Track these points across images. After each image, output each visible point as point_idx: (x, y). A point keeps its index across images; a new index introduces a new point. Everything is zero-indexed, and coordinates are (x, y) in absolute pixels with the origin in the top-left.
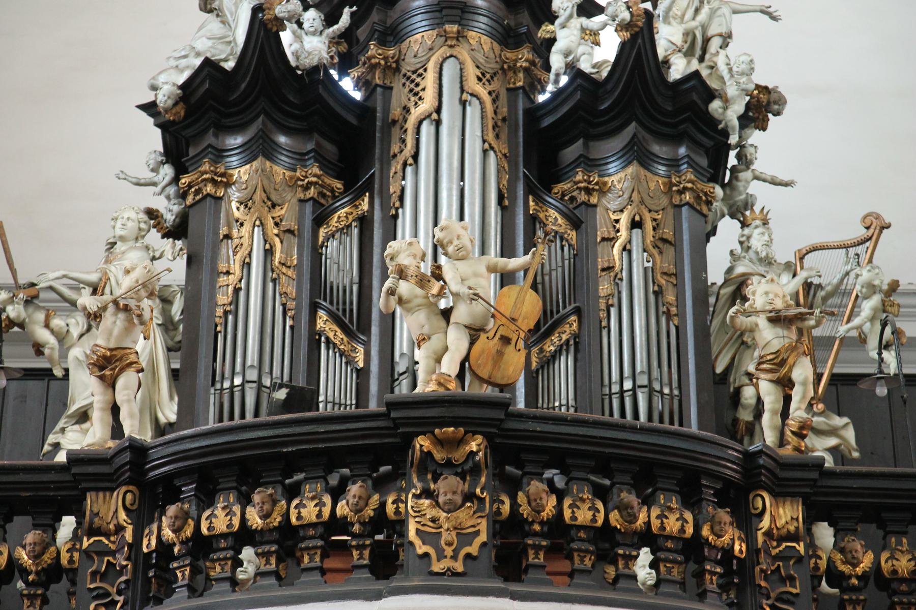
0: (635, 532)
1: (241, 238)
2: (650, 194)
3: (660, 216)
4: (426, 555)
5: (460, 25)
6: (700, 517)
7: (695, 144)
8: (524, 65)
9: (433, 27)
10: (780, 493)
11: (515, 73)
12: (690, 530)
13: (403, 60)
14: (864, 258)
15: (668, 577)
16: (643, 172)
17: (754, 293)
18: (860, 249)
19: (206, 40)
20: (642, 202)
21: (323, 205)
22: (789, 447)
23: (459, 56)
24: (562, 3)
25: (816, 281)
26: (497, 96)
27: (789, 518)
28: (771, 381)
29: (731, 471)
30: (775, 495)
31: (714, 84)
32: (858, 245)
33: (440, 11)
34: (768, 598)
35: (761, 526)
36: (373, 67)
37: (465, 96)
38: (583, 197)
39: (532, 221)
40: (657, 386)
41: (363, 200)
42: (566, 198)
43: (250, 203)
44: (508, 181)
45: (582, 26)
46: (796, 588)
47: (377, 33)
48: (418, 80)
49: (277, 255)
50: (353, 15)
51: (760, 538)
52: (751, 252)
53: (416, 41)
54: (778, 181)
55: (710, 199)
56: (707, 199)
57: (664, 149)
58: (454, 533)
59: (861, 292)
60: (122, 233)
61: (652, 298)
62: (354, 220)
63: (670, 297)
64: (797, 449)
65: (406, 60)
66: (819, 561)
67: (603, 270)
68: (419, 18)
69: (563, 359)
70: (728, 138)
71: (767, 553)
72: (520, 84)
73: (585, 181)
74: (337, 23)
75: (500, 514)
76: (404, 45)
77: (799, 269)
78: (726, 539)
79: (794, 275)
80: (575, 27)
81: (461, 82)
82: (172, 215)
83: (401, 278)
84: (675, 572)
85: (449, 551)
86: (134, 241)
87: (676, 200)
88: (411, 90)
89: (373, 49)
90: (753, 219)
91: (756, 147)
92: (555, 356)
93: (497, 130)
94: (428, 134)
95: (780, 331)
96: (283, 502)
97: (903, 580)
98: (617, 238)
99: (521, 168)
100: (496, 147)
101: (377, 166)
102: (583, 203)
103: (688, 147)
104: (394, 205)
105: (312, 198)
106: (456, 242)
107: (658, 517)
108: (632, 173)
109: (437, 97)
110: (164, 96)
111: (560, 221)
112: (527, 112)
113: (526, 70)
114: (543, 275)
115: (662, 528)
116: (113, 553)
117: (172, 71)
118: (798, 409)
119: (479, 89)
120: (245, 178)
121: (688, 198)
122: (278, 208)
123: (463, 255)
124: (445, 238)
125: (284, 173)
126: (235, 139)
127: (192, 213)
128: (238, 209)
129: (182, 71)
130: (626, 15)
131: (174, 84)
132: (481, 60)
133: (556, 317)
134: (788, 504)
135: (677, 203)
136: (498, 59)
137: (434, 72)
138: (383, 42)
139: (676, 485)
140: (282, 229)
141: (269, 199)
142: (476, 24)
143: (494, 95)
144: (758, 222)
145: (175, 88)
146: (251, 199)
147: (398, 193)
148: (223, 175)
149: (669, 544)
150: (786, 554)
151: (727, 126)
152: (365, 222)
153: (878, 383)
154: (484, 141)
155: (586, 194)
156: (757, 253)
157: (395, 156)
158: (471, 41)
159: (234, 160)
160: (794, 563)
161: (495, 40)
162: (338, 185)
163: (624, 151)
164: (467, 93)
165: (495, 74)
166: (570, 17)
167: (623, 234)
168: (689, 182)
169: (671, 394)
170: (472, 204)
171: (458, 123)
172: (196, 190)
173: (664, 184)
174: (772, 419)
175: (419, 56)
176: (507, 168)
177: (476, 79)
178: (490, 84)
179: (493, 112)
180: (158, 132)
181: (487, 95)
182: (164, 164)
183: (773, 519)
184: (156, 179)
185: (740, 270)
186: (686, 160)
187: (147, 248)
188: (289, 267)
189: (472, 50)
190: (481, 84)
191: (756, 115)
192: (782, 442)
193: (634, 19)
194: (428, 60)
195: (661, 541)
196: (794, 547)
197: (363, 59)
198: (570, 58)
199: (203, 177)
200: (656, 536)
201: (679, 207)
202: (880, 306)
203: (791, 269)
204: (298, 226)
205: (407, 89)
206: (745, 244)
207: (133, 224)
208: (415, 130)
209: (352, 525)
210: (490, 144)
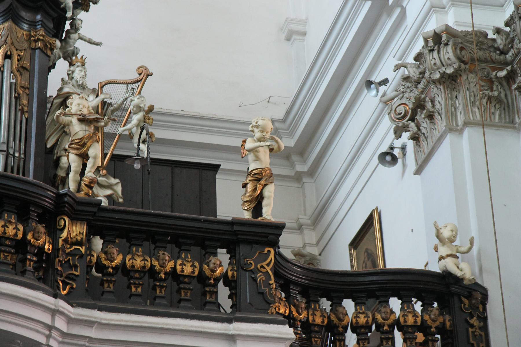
2: (18, 40)
3: (22, 54)
6: (27, 228)
7: (46, 14)
10: (74, 219)
12: (20, 235)
14: (136, 91)
15: (5, 261)
16: (14, 26)
17: (71, 104)
18: (134, 86)
20: (12, 44)
22: (83, 193)
25: (109, 101)
27: (78, 233)
28: (76, 155)
29: (48, 203)
30: (72, 219)
32: (134, 83)
34: (61, 276)
35: (62, 236)
40: (11, 152)
46: (78, 272)
52: (73, 80)
54: (93, 41)
55: (52, 47)
56: (51, 47)
57: (28, 15)
59: (133, 109)
61: (13, 100)
63: (24, 101)
64: (87, 194)
66: (92, 258)
70: (66, 13)
71: (64, 251)
77: (100, 93)
78: (41, 242)
79: (97, 96)
84: (9, 258)
87: (33, 45)
90: (77, 62)
91: (82, 21)
95: (84, 127)
97: (137, 271)
103: (42, 16)
108: (7, 27)
118: (90, 172)
121: (40, 45)
134: (78, 225)
135: (33, 47)
139: (15, 209)
144: (79, 64)
149: (8, 242)
150: (74, 253)
151: (65, 6)
153: (136, 162)
156: (77, 81)
160: (78, 258)
163: (4, 13)
168: (41, 35)
169: (19, 157)
173: (26, 35)
174: (74, 176)
183: (69, 232)
185: (66, 90)
186: (40, 23)
191: (83, 2)
192: (79, 190)
196: (79, 249)
201: (34, 49)
202: (143, 119)
206: (70, 76)
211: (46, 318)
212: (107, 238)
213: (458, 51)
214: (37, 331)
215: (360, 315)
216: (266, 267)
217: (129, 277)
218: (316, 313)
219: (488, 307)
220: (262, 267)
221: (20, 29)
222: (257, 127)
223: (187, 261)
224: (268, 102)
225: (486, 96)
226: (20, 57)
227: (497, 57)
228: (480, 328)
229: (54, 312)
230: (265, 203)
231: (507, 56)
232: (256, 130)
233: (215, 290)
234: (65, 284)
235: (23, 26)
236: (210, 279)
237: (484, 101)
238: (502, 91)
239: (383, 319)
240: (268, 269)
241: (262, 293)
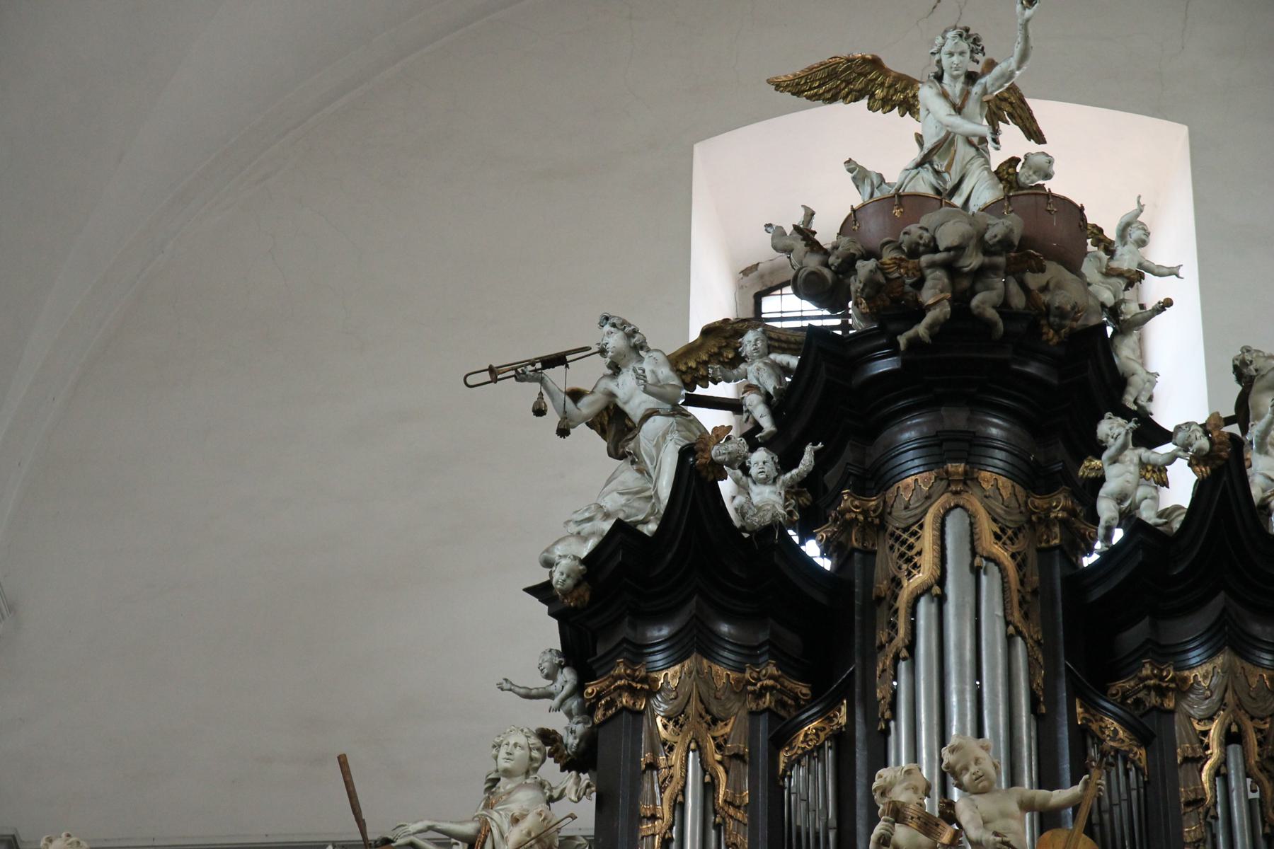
1: (670, 767)
2: (1252, 694)
3: (1268, 726)
5: (967, 463)
8: (1060, 515)
9: (929, 467)
11: (1047, 527)
13: (890, 513)
16: (1238, 662)
19: (618, 495)
20: (1240, 705)
21: (783, 719)
23: (968, 506)
24: (1111, 429)
26: (1024, 560)
33: (940, 445)
36: (847, 525)
37: (978, 561)
38: (1154, 699)
39: (1082, 736)
41: (839, 711)
42: (1129, 702)
43: (682, 719)
44: (1044, 680)
45: (1140, 459)
47: (852, 478)
48: (912, 540)
49: (722, 791)
50: (817, 454)
53: (908, 486)
57: (1269, 629)
60: (508, 765)
62: (827, 739)
65: (894, 514)
67: (1188, 804)
68: (910, 455)
72: (1057, 541)
73: (1155, 676)
74: (797, 466)
80: (1131, 461)
81: (972, 542)
82: (575, 738)
83: (897, 821)
86: (524, 777)
88: (902, 555)
89: (847, 500)
93: (1025, 607)
98: (1207, 758)
99: (1063, 662)
100: (1025, 631)
101: (857, 661)
102: (1154, 708)
104: (883, 716)
105: (768, 709)
106: (973, 769)
108: (1223, 664)
109: (939, 563)
110: (562, 574)
111: (1121, 734)
112: (1066, 580)
113: (1063, 523)
114: (1100, 812)
117: (572, 540)
119: (997, 550)
120: (674, 683)
122: (721, 724)
123: (984, 787)
124: (957, 763)
125: (727, 674)
126: (660, 630)
127: (601, 734)
128: (665, 726)
129: (585, 539)
130: (1204, 443)
131: (575, 558)
132: (999, 511)
136: (1023, 509)
137: (933, 529)
138: (861, 491)
140: (727, 753)
141: (708, 711)
142: (990, 461)
143: (1019, 558)
145: (577, 563)
146: (683, 712)
147: (888, 699)
148: (644, 680)
152: (842, 741)
154: (1007, 623)
155: (1157, 695)
157: (882, 647)
158: (985, 485)
159: (659, 659)
161: (1017, 483)
162: (803, 689)
164: (981, 556)
165: (1019, 529)
166: (1124, 447)
167: (1215, 752)
170: (994, 713)
171: (970, 599)
172: (607, 702)
175: (911, 507)
176: (1042, 663)
177: (993, 537)
178: (1013, 544)
179: (1018, 583)
180: (556, 622)
181: (1009, 558)
182: (562, 667)
184: (552, 689)
187: (542, 785)
188: (738, 807)
189: (986, 497)
190: (1000, 544)
193: (1216, 448)
194: (925, 512)
197: (833, 515)
198: (1127, 504)
199: (616, 684)
204: (750, 749)
205: (896, 554)
207: (523, 752)
208: (909, 611)
210: (1016, 628)
221: (1254, 665)
226: (1264, 734)
235: (1259, 657)
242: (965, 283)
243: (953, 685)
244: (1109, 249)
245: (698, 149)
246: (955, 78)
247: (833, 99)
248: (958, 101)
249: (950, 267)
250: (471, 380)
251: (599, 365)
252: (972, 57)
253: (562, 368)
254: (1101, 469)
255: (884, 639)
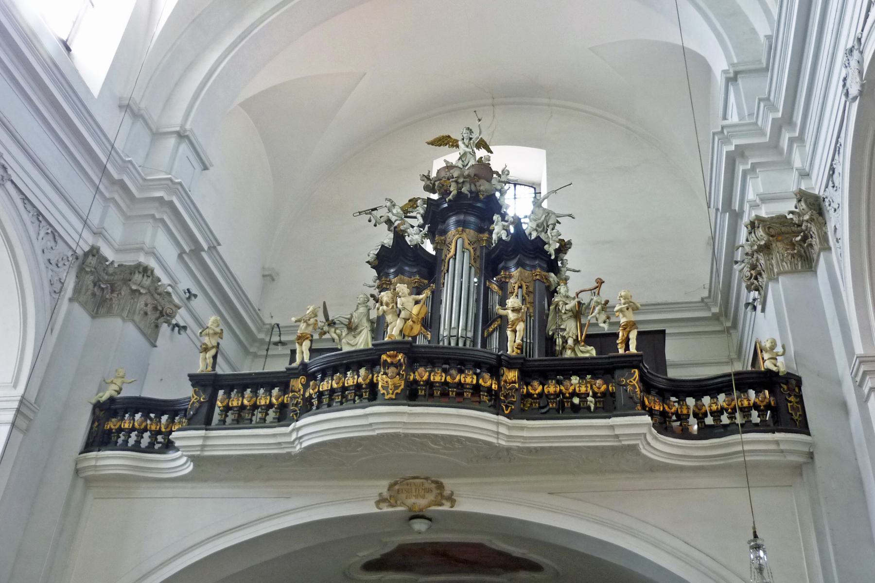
0: (455, 383)
4: (384, 394)
10: (510, 367)
11: (483, 242)
12: (475, 382)
14: (597, 293)
17: (508, 302)
18: (595, 291)
25: (583, 302)
26: (476, 249)
31: (546, 240)
34: (505, 402)
38: (503, 280)
46: (514, 398)
48: (450, 246)
50: (429, 227)
51: (502, 383)
58: (393, 386)
69: (495, 333)
71: (505, 388)
72: (484, 245)
75: (410, 379)
76: (446, 236)
85: (391, 392)
92: (493, 332)
94: (452, 263)
96: (343, 379)
97: (552, 394)
107: (464, 378)
111: (496, 288)
113: (486, 240)
115: (465, 381)
116: (298, 398)
118: (518, 339)
129: (377, 249)
133: (492, 320)
154: (470, 264)
156: (562, 294)
157: (442, 271)
169: (530, 343)
187: (367, 306)
194: (453, 239)
195: (465, 386)
198: (499, 235)
200: (463, 384)
203: (574, 298)
209: (363, 384)
211: (493, 428)
212: (712, 396)
213: (767, 229)
214: (489, 436)
215: (713, 405)
216: (633, 381)
217: (647, 409)
218: (683, 407)
219: (802, 388)
220: (631, 382)
222: (621, 297)
223: (583, 384)
224: (704, 288)
225: (789, 254)
227: (796, 229)
228: (796, 403)
229: (498, 424)
230: (630, 342)
231: (803, 227)
232: (621, 299)
233: (750, 413)
234: (507, 407)
236: (598, 393)
237: (790, 257)
238: (801, 249)
239: (727, 405)
240: (634, 382)
241: (631, 398)
242: (460, 185)
243: (456, 278)
244: (499, 176)
245: (434, 161)
246: (467, 139)
247: (440, 145)
248: (467, 144)
249: (457, 182)
250: (354, 215)
251: (386, 210)
252: (470, 134)
253: (376, 211)
254: (494, 227)
255: (443, 269)
